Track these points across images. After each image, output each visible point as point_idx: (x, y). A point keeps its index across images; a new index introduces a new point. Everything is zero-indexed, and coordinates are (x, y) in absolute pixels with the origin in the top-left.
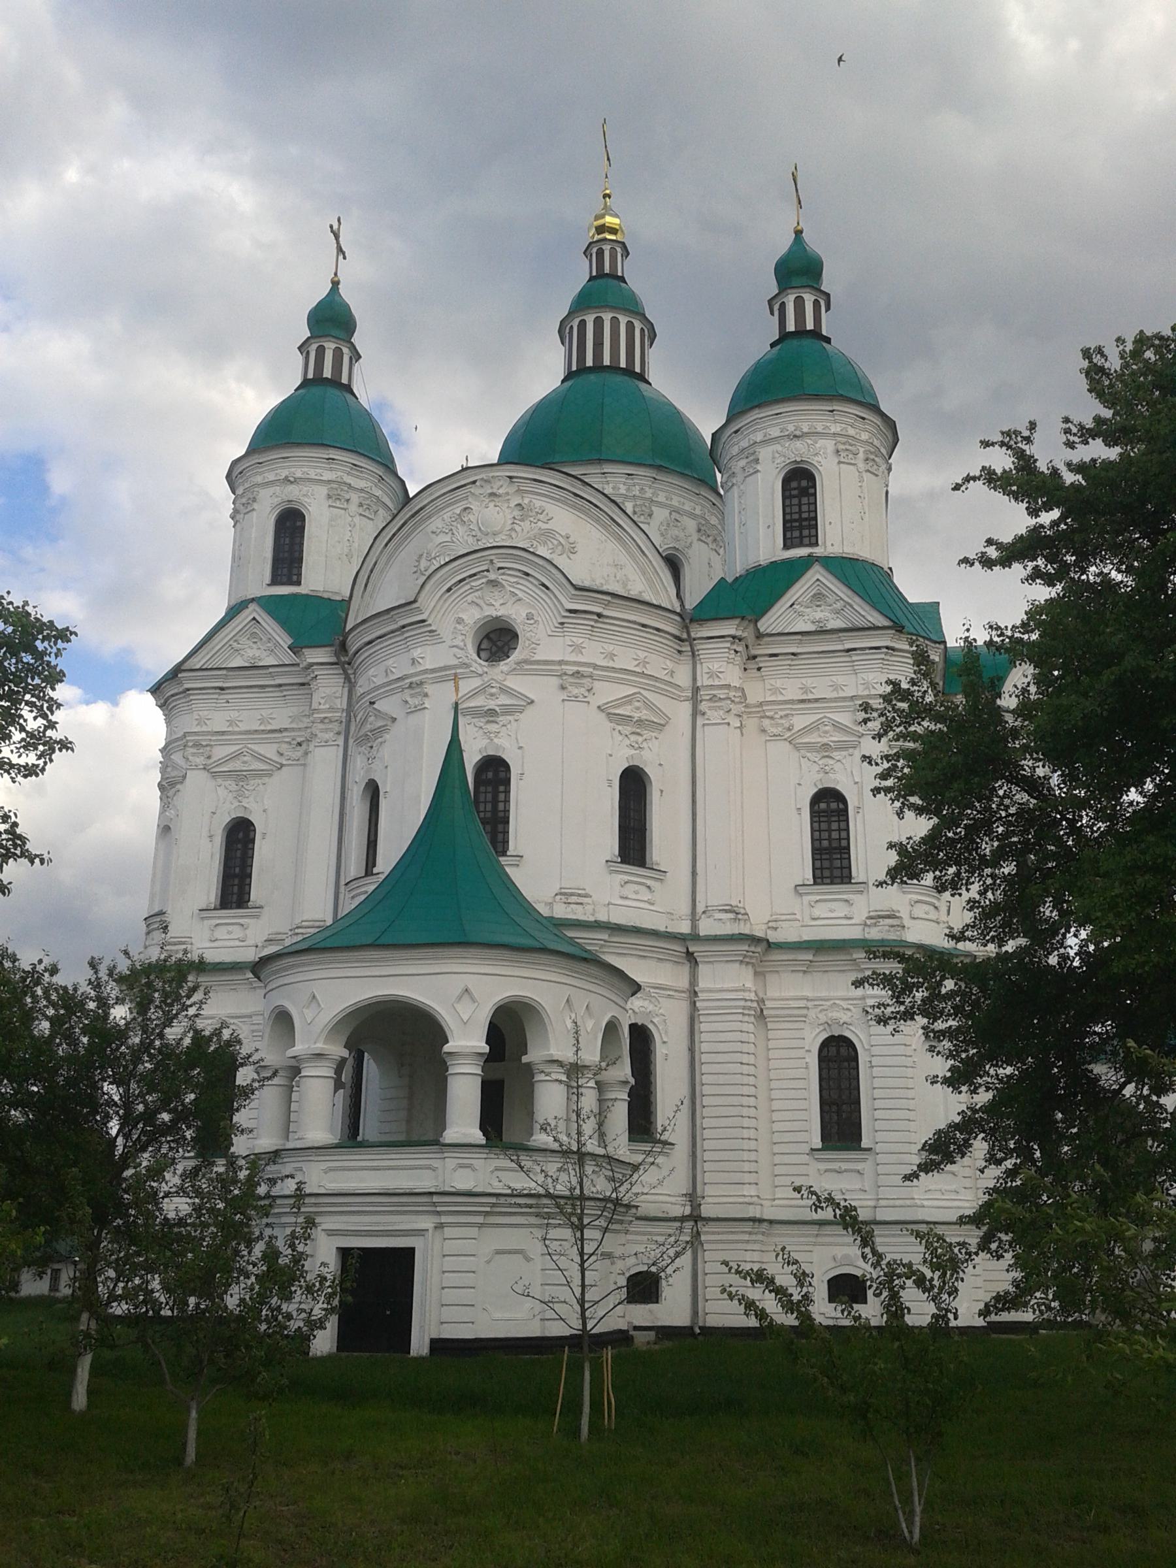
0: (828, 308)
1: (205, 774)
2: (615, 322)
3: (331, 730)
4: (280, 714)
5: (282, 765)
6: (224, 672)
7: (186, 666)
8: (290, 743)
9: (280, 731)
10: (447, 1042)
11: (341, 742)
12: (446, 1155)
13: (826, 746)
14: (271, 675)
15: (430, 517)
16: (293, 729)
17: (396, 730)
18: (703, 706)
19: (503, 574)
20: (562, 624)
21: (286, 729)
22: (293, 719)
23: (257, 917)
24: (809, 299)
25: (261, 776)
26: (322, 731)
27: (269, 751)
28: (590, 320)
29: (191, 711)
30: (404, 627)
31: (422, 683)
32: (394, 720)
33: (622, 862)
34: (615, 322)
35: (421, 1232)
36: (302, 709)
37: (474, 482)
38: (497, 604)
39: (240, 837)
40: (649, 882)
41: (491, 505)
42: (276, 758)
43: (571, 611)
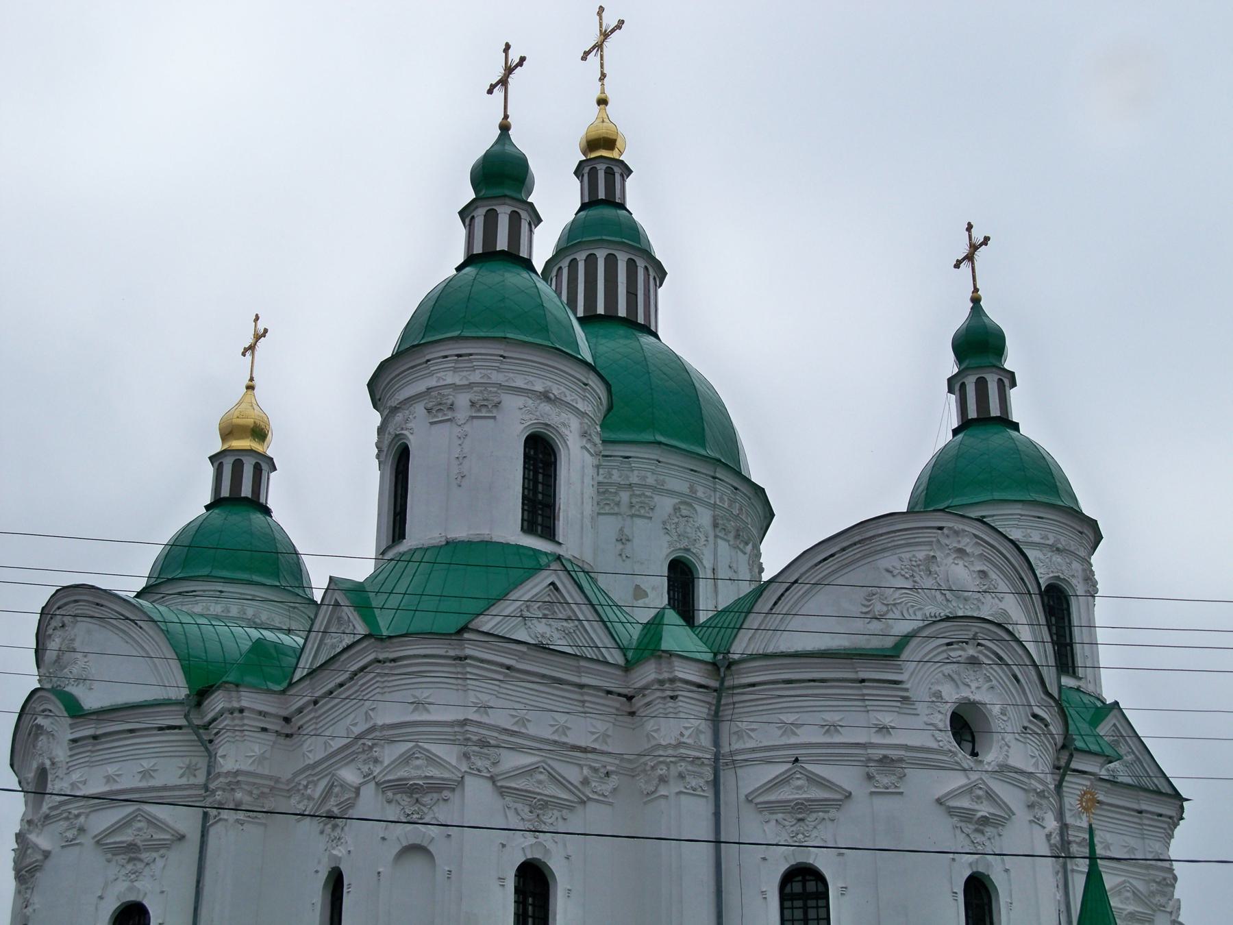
1: (488, 785)
2: (611, 261)
3: (701, 775)
8: (595, 770)
9: (584, 750)
14: (579, 670)
15: (884, 550)
19: (980, 652)
20: (1025, 728)
21: (594, 751)
30: (863, 681)
31: (901, 760)
32: (849, 796)
34: (611, 261)
37: (941, 528)
38: (974, 685)
41: (961, 563)
43: (1035, 716)
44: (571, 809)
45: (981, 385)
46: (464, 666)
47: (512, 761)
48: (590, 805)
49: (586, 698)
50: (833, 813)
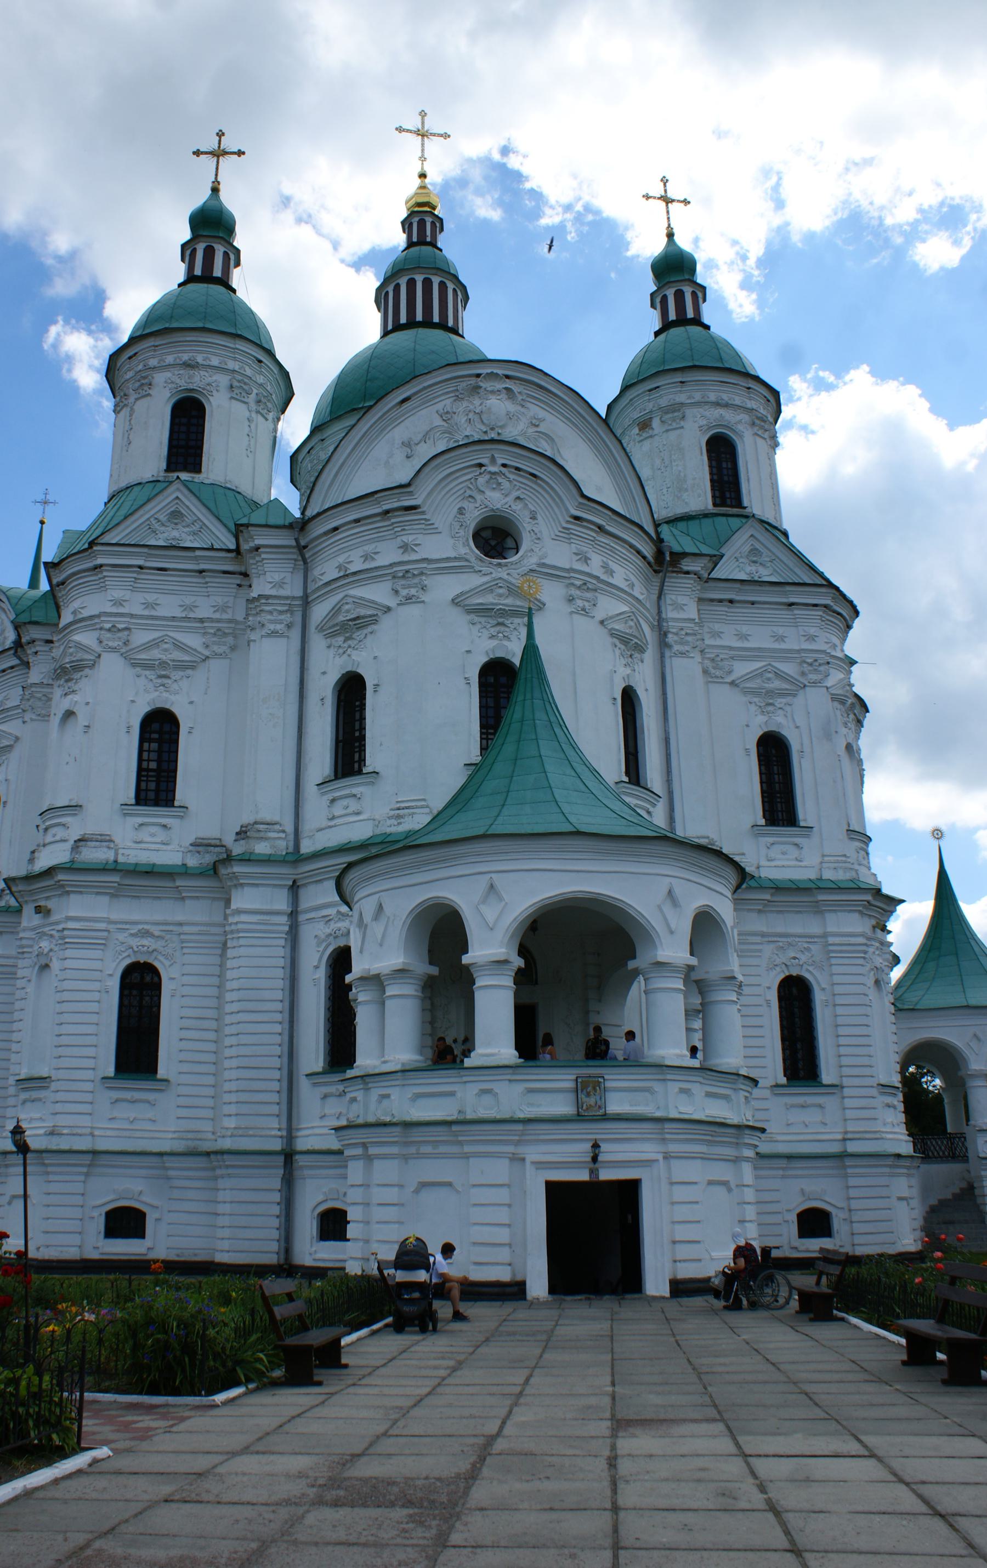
0: (704, 300)
4: (210, 602)
5: (208, 657)
6: (146, 550)
7: (100, 541)
10: (634, 957)
11: (296, 634)
12: (669, 1077)
13: (770, 693)
16: (218, 621)
17: (386, 622)
18: (671, 638)
22: (217, 609)
23: (182, 817)
24: (688, 291)
25: (187, 668)
26: (271, 622)
27: (194, 641)
28: (419, 279)
29: (104, 588)
33: (630, 783)
35: (648, 1163)
36: (226, 599)
39: (160, 730)
40: (651, 809)
42: (200, 649)
44: (193, 668)
45: (679, 295)
46: (101, 572)
47: (140, 637)
48: (211, 661)
49: (208, 580)
50: (369, 629)
